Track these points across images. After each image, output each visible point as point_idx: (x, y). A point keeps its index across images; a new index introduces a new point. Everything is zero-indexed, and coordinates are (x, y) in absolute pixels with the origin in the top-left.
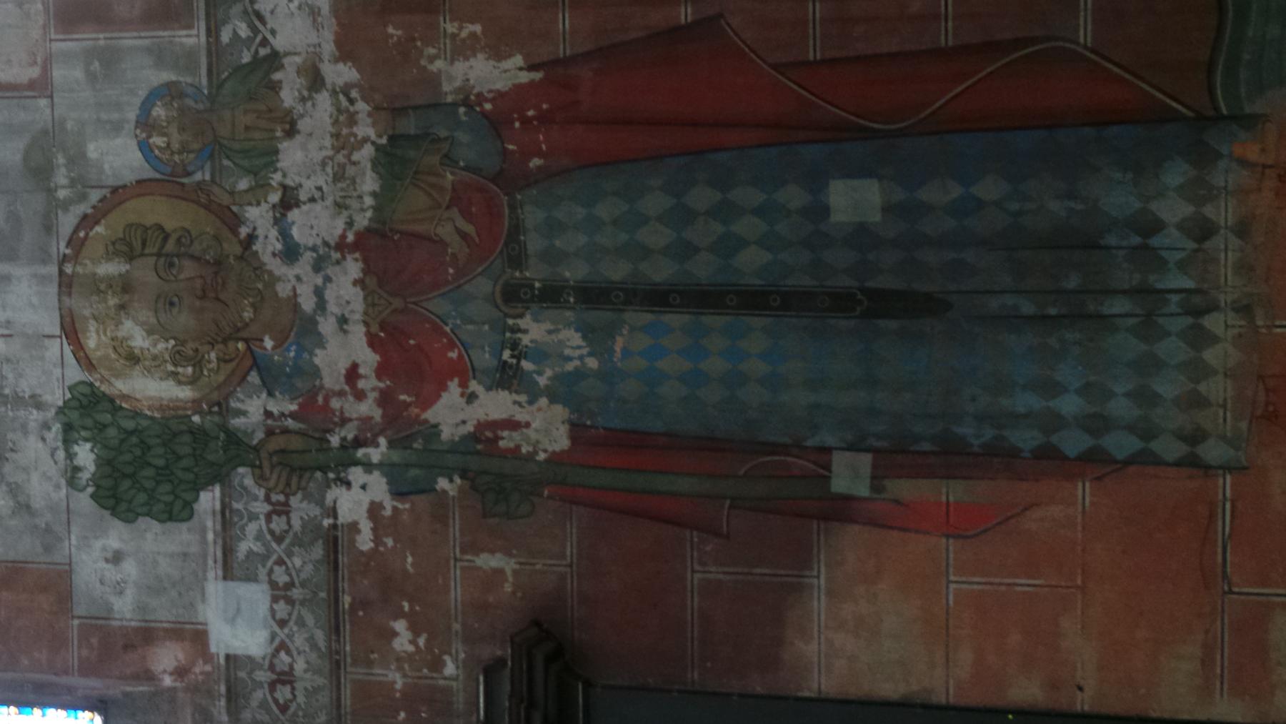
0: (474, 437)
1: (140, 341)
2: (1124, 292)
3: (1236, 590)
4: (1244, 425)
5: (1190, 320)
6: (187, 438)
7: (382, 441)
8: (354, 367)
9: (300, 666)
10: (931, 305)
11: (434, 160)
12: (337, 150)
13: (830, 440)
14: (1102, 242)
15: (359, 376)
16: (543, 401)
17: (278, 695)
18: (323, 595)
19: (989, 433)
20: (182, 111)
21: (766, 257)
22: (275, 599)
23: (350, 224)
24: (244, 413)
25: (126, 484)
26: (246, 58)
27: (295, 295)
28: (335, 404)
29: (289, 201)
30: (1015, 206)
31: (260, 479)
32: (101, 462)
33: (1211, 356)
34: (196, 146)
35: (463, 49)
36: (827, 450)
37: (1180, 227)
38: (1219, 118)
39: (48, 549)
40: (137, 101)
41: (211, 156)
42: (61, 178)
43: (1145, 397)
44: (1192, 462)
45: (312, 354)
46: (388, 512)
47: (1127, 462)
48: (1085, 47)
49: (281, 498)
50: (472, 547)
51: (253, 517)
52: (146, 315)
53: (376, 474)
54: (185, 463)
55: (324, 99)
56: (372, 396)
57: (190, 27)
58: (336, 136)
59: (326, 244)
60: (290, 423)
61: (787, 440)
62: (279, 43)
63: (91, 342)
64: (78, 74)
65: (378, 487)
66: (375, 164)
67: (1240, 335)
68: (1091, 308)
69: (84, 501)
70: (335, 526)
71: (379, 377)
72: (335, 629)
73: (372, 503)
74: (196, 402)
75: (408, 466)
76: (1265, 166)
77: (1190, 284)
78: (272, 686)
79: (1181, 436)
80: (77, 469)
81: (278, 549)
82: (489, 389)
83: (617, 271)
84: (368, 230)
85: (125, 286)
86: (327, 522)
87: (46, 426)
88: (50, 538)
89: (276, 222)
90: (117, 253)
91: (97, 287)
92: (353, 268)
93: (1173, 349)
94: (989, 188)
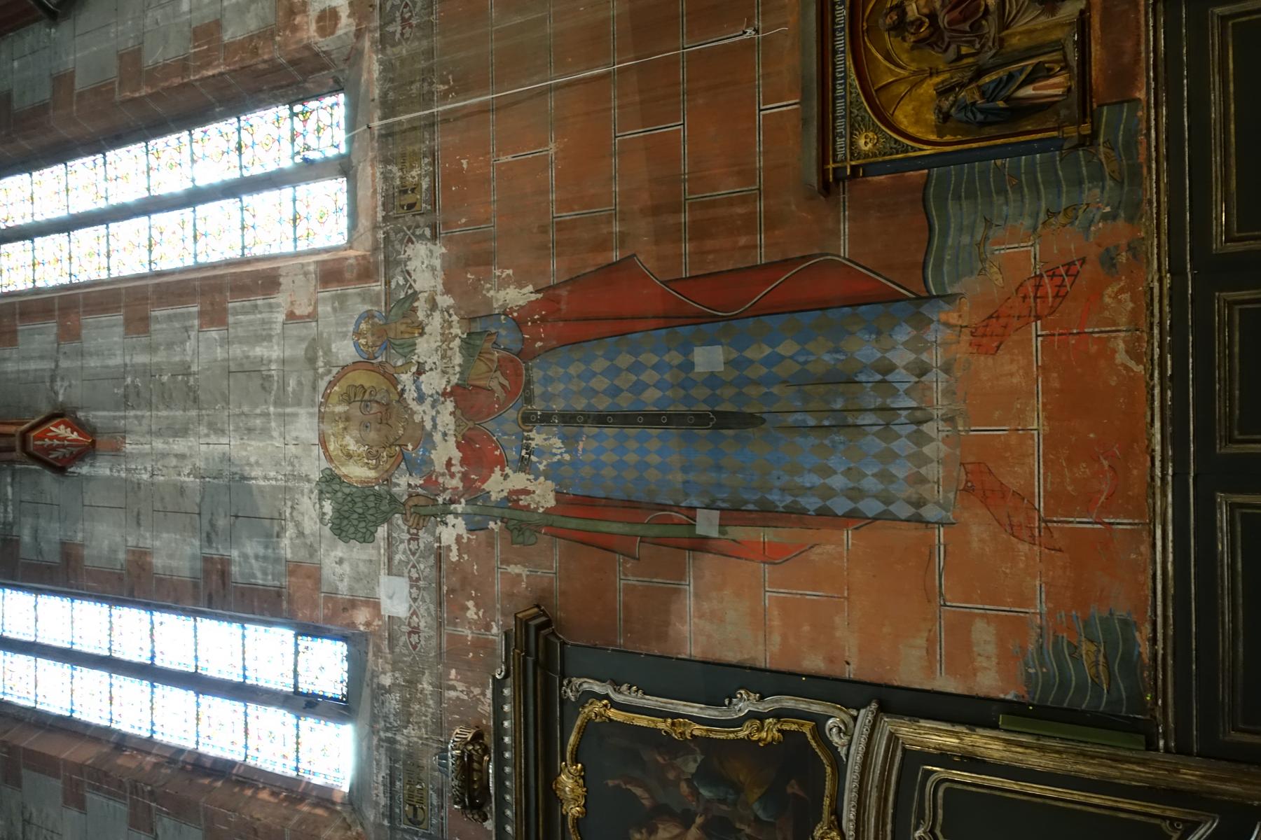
0: (507, 499)
1: (352, 447)
2: (871, 410)
3: (948, 604)
4: (951, 496)
5: (914, 427)
6: (372, 498)
7: (463, 500)
8: (450, 459)
9: (422, 624)
11: (488, 345)
12: (443, 342)
13: (695, 503)
14: (857, 379)
15: (452, 465)
16: (542, 479)
17: (412, 639)
18: (434, 585)
20: (373, 325)
21: (658, 394)
22: (411, 587)
23: (448, 382)
24: (398, 485)
25: (345, 522)
27: (423, 421)
28: (441, 480)
30: (802, 359)
31: (405, 520)
32: (336, 510)
33: (927, 450)
34: (379, 343)
35: (504, 284)
36: (695, 508)
37: (906, 368)
38: (931, 297)
39: (311, 556)
40: (354, 321)
41: (386, 348)
42: (320, 363)
43: (886, 477)
44: (918, 519)
45: (430, 453)
46: (465, 540)
47: (875, 519)
48: (844, 258)
49: (415, 531)
50: (506, 562)
51: (402, 542)
52: (356, 433)
53: (460, 518)
54: (371, 512)
55: (437, 315)
56: (459, 475)
57: (377, 281)
58: (442, 334)
59: (437, 393)
60: (419, 490)
61: (672, 503)
62: (417, 287)
63: (331, 447)
64: (329, 309)
66: (461, 348)
67: (947, 436)
68: (850, 420)
69: (327, 531)
70: (440, 547)
71: (462, 466)
72: (440, 604)
73: (458, 535)
76: (961, 327)
77: (914, 404)
80: (324, 514)
82: (515, 472)
83: (580, 405)
84: (457, 385)
86: (436, 545)
87: (311, 492)
88: (312, 550)
89: (415, 381)
90: (343, 401)
91: (335, 418)
92: (450, 406)
93: (903, 445)
94: (787, 348)
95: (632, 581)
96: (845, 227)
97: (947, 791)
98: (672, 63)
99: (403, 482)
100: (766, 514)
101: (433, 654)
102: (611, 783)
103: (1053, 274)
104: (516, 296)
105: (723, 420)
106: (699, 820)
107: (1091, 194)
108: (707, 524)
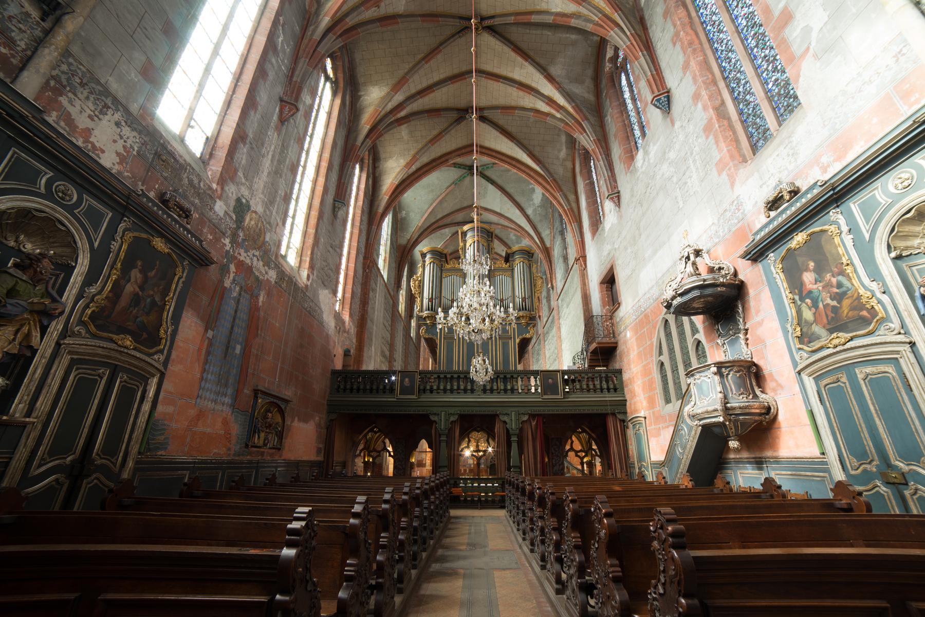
10: (225, 357)
19: (209, 361)
29: (258, 260)
35: (264, 297)
55: (264, 273)
65: (228, 248)
69: (240, 195)
74: (244, 225)
79: (202, 395)
85: (257, 226)
91: (258, 221)
94: (235, 371)
95: (204, 302)
96: (248, 392)
97: (135, 389)
100: (208, 353)
102: (158, 262)
103: (230, 437)
104: (261, 299)
105: (227, 348)
106: (140, 293)
107: (238, 447)
108: (210, 334)
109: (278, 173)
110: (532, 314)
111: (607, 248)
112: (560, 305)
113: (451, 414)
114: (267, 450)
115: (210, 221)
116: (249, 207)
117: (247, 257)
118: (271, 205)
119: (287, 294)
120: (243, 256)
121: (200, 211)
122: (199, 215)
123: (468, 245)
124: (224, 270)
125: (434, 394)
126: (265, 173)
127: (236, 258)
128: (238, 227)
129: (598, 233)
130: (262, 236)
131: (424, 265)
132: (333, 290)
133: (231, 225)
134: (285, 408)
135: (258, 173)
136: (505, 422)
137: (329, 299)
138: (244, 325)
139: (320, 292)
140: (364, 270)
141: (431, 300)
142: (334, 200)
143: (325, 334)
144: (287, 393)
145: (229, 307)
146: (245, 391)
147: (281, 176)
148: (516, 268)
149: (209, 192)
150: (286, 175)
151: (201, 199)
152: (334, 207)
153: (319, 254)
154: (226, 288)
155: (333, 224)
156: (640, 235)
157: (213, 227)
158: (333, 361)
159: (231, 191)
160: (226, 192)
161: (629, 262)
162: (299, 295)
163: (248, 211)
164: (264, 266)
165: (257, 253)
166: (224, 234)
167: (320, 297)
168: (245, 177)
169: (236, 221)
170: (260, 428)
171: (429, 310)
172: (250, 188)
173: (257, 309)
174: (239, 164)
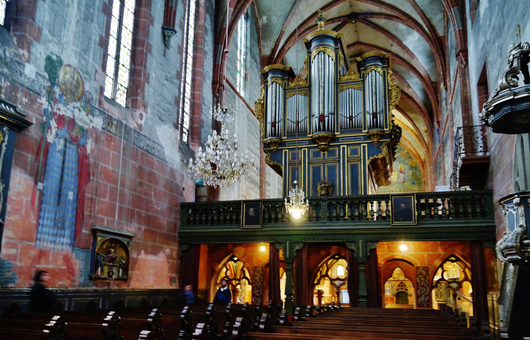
0: (50, 126)
11: (81, 135)
22: (32, 80)
26: (94, 112)
29: (80, 110)
31: (49, 86)
35: (91, 144)
50: (36, 119)
55: (89, 121)
62: (95, 118)
66: (82, 126)
69: (49, 53)
72: (27, 88)
74: (59, 81)
75: (48, 113)
78: (20, 72)
81: (39, 84)
85: (73, 78)
87: (59, 53)
88: (45, 43)
91: (74, 73)
92: (72, 117)
98: (116, 200)
99: (57, 90)
101: (14, 78)
109: (88, 18)
110: (384, 132)
111: (482, 39)
112: (453, 110)
113: (296, 242)
114: (112, 282)
115: (22, 85)
116: (61, 62)
117: (67, 111)
118: (85, 54)
119: (118, 138)
120: (64, 110)
121: (10, 79)
122: (11, 83)
123: (312, 57)
124: (45, 127)
125: (279, 222)
126: (74, 23)
127: (56, 114)
128: (53, 84)
129: (475, 20)
130: (81, 88)
131: (267, 86)
132: (174, 124)
133: (45, 85)
134: (128, 243)
135: (65, 25)
136: (352, 251)
137: (170, 133)
138: (74, 173)
139: (158, 128)
140: (214, 95)
141: (274, 124)
142: (163, 29)
143: (169, 169)
144: (129, 229)
145: (55, 160)
146: (84, 231)
147: (92, 21)
148: (367, 79)
149: (17, 59)
150: (98, 18)
151: (9, 68)
152: (164, 36)
153: (151, 90)
154: (49, 143)
155: (165, 55)
156: (504, 24)
157: (27, 90)
158: (182, 195)
159: (39, 51)
160: (33, 54)
161: (497, 60)
162: (132, 136)
163: (60, 67)
164: (87, 115)
165: (78, 104)
166: (39, 94)
167: (158, 133)
168: (51, 34)
169: (50, 80)
170: (103, 263)
171: (272, 135)
172: (59, 43)
173: (86, 157)
174: (43, 23)
